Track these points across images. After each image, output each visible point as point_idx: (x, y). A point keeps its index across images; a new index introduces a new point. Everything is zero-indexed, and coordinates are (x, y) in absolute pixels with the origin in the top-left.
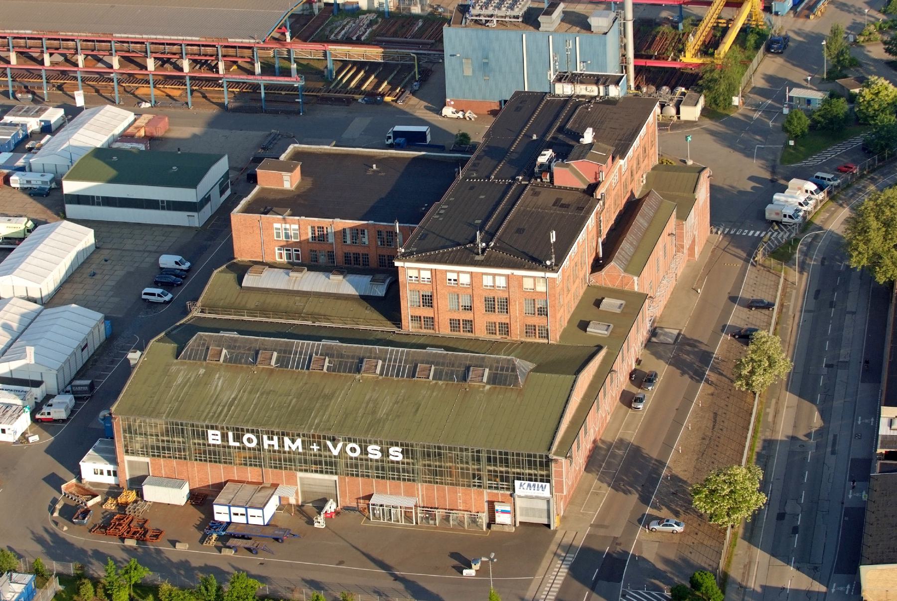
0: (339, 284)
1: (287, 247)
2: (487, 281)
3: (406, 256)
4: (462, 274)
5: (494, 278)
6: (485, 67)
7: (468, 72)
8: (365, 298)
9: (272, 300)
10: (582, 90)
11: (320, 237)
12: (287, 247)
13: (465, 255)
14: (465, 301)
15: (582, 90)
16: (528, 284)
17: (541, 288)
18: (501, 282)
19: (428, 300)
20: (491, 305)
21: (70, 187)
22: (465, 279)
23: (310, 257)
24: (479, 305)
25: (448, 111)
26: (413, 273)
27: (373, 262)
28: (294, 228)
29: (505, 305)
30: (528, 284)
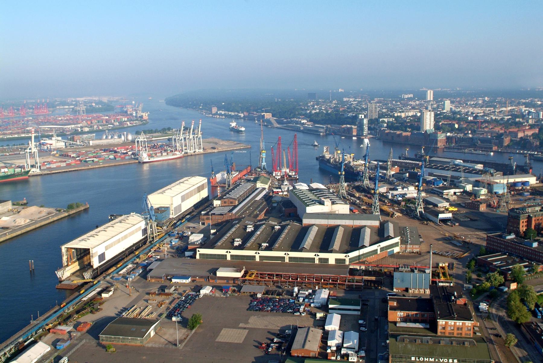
0: (418, 325)
1: (400, 318)
2: (458, 324)
3: (439, 319)
4: (451, 322)
5: (459, 323)
6: (402, 281)
7: (399, 282)
8: (425, 328)
9: (405, 329)
10: (444, 284)
11: (408, 316)
12: (400, 318)
13: (452, 319)
14: (452, 328)
15: (444, 284)
16: (467, 324)
17: (470, 325)
18: (461, 324)
19: (444, 328)
20: (458, 329)
21: (330, 306)
22: (453, 324)
23: (405, 320)
24: (456, 329)
25: (395, 290)
26: (441, 322)
27: (420, 321)
28: (401, 314)
29: (462, 328)
30: (467, 324)
